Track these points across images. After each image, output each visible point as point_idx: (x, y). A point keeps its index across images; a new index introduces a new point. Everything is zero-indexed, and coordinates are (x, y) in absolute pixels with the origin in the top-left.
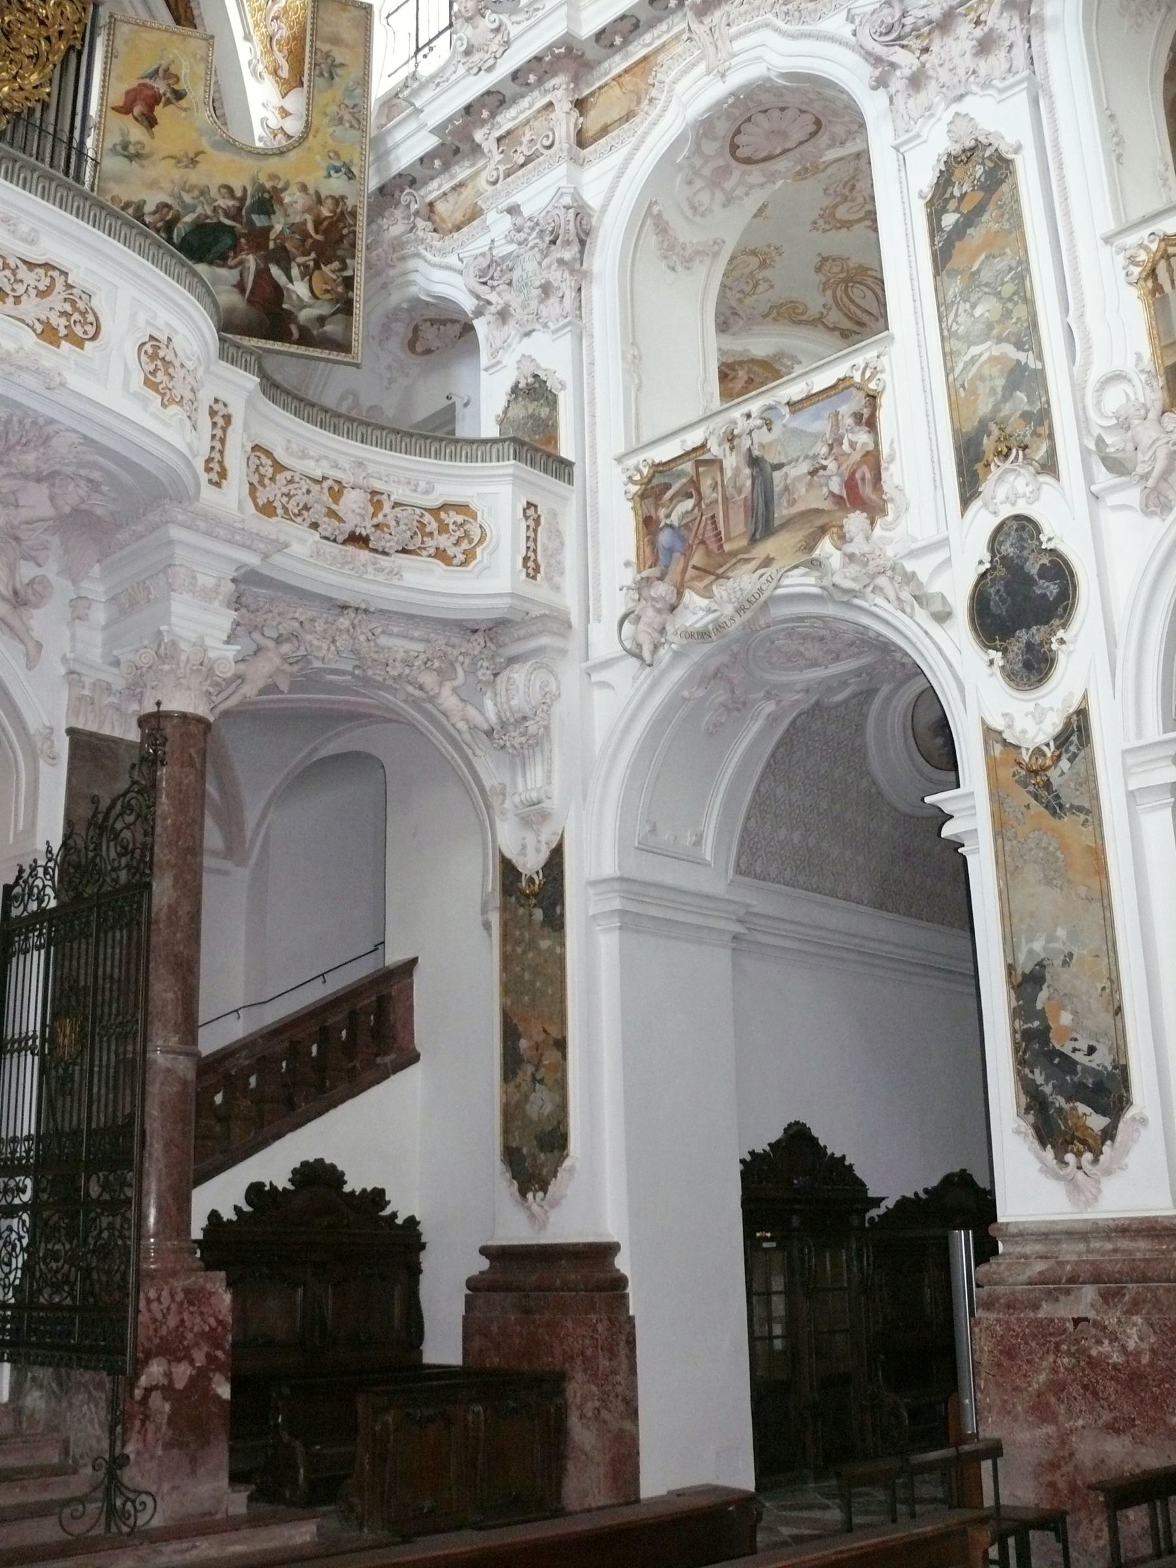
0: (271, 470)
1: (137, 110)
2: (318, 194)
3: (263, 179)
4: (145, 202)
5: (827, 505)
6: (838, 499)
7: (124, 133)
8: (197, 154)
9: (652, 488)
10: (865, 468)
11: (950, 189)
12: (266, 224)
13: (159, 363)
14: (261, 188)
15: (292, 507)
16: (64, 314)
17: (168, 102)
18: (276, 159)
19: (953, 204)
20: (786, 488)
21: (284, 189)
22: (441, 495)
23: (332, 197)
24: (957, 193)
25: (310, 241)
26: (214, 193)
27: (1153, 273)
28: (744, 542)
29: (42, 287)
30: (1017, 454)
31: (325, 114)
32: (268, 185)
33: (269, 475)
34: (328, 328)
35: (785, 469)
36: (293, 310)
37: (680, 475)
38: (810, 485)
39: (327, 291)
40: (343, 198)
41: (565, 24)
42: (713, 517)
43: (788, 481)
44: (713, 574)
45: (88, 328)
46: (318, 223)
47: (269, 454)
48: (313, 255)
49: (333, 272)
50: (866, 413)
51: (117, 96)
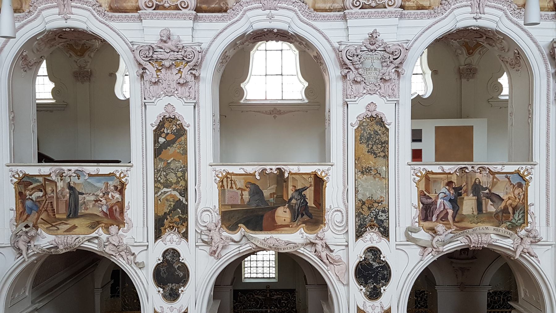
5: (100, 214)
6: (105, 214)
9: (23, 181)
10: (117, 207)
11: (163, 129)
19: (163, 135)
20: (84, 203)
24: (165, 132)
27: (222, 181)
28: (65, 217)
30: (176, 229)
35: (84, 196)
37: (37, 181)
38: (94, 205)
42: (51, 203)
43: (85, 201)
44: (49, 223)
50: (119, 187)
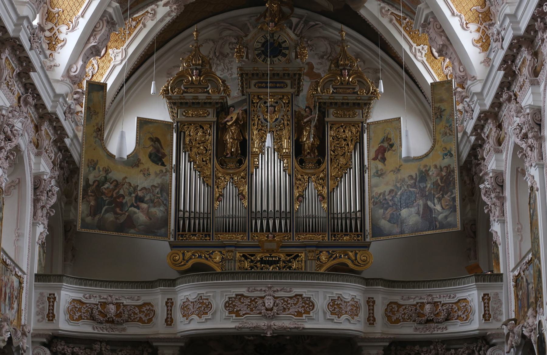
0: (397, 308)
1: (379, 157)
2: (440, 167)
3: (422, 168)
4: (385, 191)
7: (376, 168)
8: (400, 167)
12: (424, 186)
13: (336, 306)
14: (421, 172)
15: (406, 317)
16: (303, 307)
17: (389, 150)
18: (426, 158)
21: (429, 170)
22: (458, 297)
23: (445, 167)
25: (440, 187)
26: (406, 179)
29: (295, 302)
31: (440, 133)
32: (424, 170)
33: (396, 310)
34: (449, 219)
36: (436, 216)
39: (447, 205)
40: (449, 165)
41: (479, 108)
45: (311, 307)
46: (441, 179)
47: (395, 303)
48: (441, 192)
49: (448, 197)
51: (373, 155)
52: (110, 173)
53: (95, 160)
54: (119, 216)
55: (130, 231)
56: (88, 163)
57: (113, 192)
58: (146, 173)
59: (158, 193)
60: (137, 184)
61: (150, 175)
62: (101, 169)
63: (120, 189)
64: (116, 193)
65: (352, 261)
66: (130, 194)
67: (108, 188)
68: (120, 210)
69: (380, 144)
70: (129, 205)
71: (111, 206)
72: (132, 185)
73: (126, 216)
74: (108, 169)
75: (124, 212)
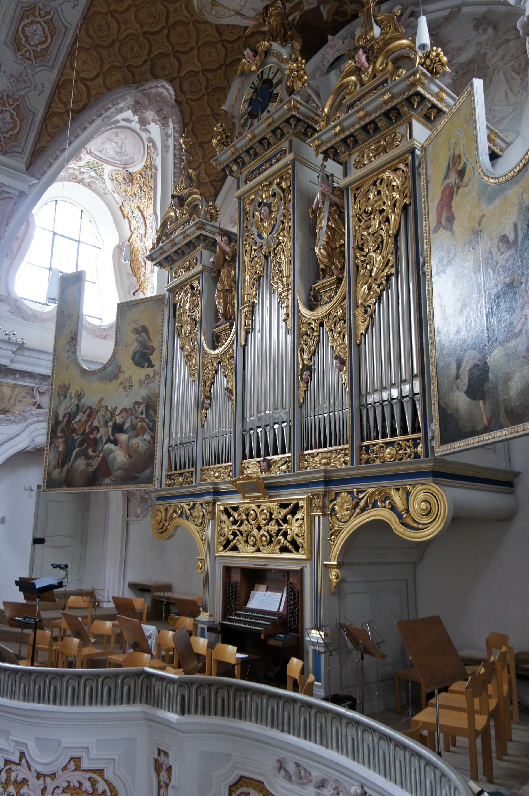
17: (458, 188)
52: (82, 398)
53: (67, 384)
54: (91, 460)
55: (104, 482)
56: (59, 390)
57: (86, 424)
58: (127, 385)
59: (142, 413)
60: (114, 407)
61: (132, 386)
62: (73, 395)
63: (94, 419)
64: (90, 427)
65: (400, 516)
66: (106, 422)
67: (80, 421)
68: (94, 451)
69: (443, 183)
70: (104, 440)
71: (82, 448)
72: (109, 409)
73: (100, 458)
74: (81, 392)
75: (97, 453)
